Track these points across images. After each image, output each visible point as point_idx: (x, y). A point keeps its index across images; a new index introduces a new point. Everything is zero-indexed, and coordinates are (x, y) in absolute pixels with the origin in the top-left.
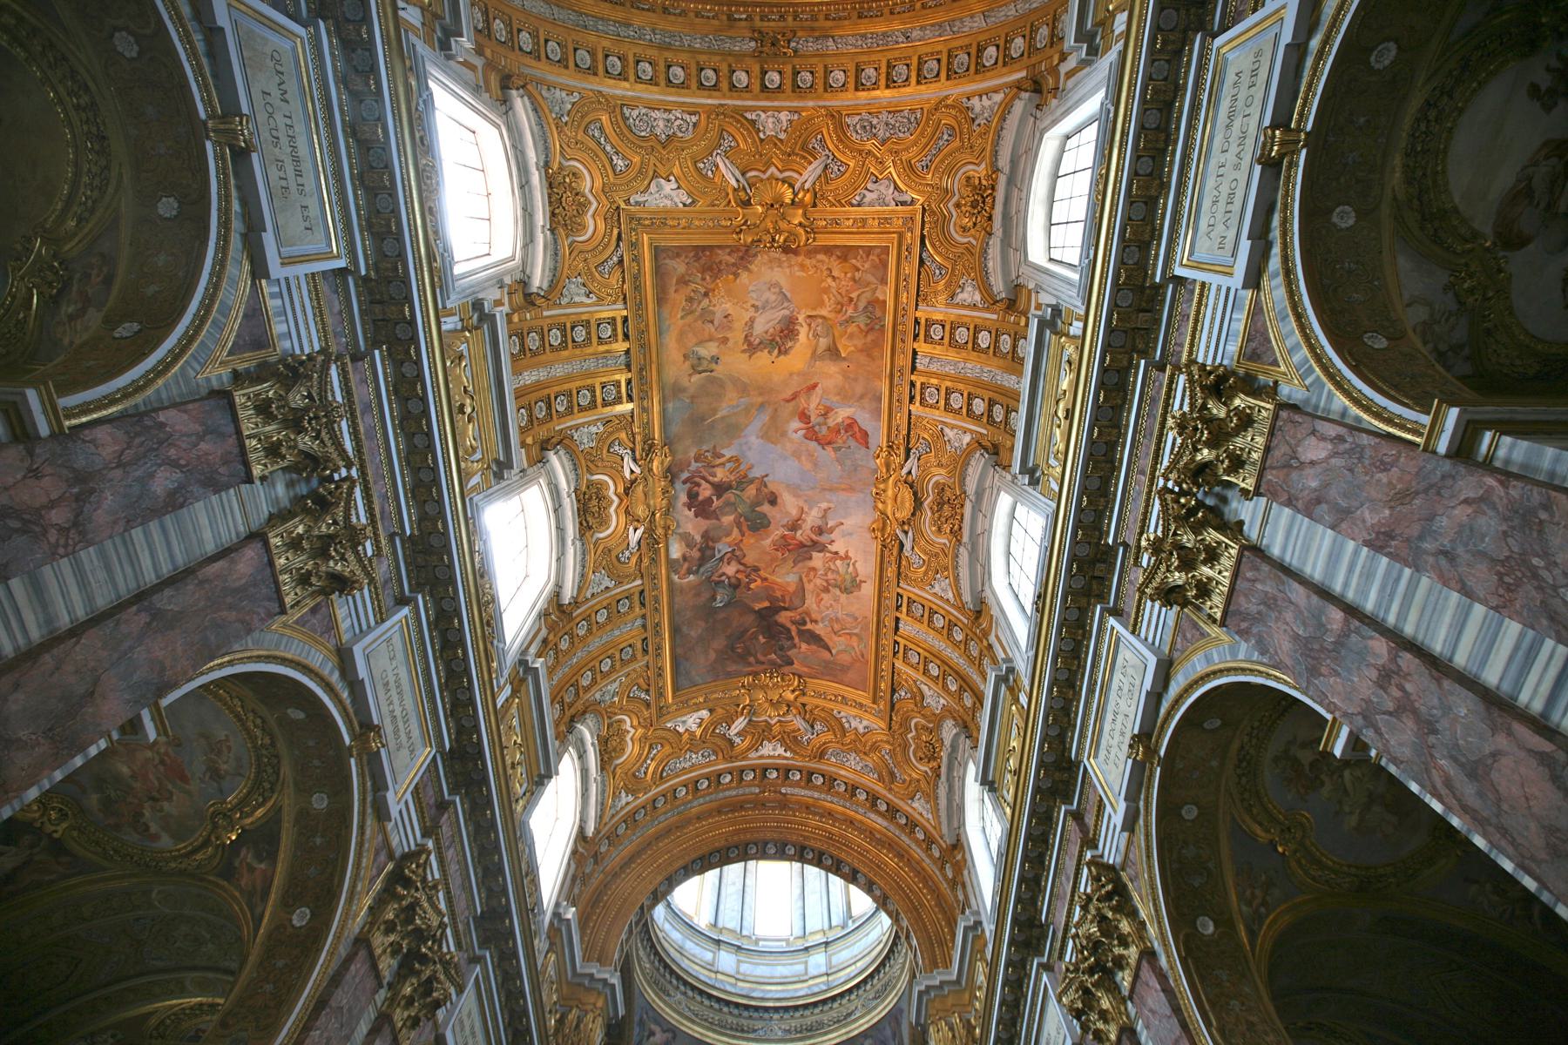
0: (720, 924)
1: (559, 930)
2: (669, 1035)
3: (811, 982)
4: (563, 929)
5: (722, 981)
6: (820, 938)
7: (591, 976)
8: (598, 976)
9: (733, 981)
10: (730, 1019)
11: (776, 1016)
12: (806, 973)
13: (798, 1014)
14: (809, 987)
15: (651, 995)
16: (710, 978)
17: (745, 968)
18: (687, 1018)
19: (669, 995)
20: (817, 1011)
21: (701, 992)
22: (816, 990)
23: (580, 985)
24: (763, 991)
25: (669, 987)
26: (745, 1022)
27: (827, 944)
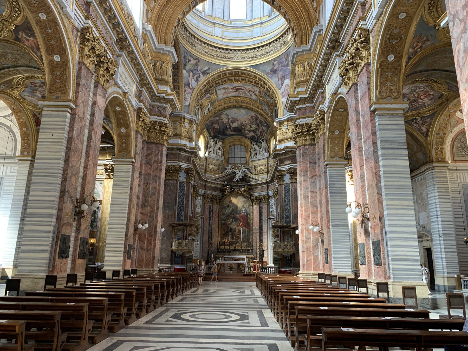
0: (214, 16)
1: (146, 34)
2: (197, 61)
3: (254, 39)
4: (148, 33)
5: (216, 40)
6: (258, 21)
7: (163, 49)
8: (165, 49)
9: (221, 39)
10: (220, 54)
11: (239, 53)
12: (252, 36)
13: (248, 52)
14: (253, 41)
15: (187, 47)
16: (211, 38)
17: (226, 34)
18: (203, 54)
19: (195, 46)
20: (256, 50)
21: (208, 44)
22: (256, 43)
23: (159, 52)
24: (234, 43)
25: (194, 43)
26: (227, 55)
27: (261, 23)
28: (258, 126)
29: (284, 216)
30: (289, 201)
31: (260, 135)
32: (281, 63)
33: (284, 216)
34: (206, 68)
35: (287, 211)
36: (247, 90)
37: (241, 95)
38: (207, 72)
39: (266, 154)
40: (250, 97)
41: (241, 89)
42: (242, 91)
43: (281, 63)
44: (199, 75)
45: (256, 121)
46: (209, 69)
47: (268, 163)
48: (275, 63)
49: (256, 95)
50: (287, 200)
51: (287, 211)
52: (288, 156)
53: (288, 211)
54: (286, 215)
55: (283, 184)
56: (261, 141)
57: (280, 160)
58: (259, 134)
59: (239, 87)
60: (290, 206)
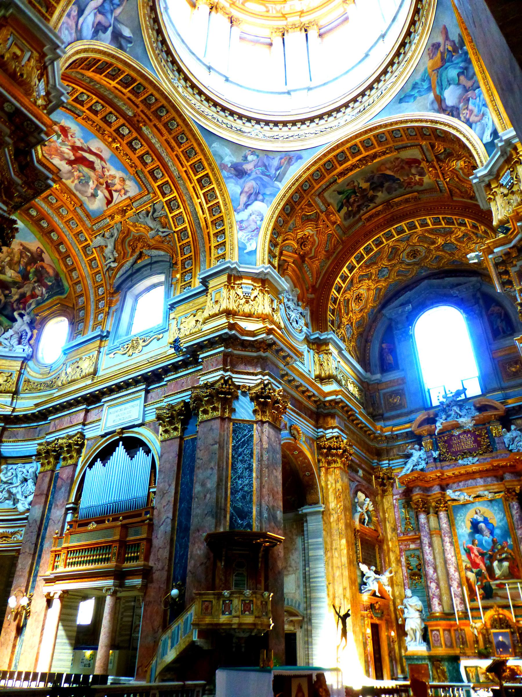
28: (25, 277)
29: (229, 509)
30: (250, 468)
31: (18, 301)
32: (265, 166)
33: (229, 509)
34: (127, 32)
35: (239, 496)
36: (103, 176)
37: (68, 182)
38: (123, 42)
39: (20, 350)
40: (84, 199)
41: (91, 165)
42: (86, 170)
43: (265, 166)
44: (107, 24)
45: (27, 264)
46: (129, 40)
47: (20, 374)
48: (250, 158)
49: (109, 202)
50: (240, 465)
51: (239, 496)
52: (255, 354)
53: (244, 497)
54: (234, 508)
55: (229, 419)
56: (16, 314)
57: (226, 355)
58: (16, 297)
59: (91, 158)
60: (250, 485)
